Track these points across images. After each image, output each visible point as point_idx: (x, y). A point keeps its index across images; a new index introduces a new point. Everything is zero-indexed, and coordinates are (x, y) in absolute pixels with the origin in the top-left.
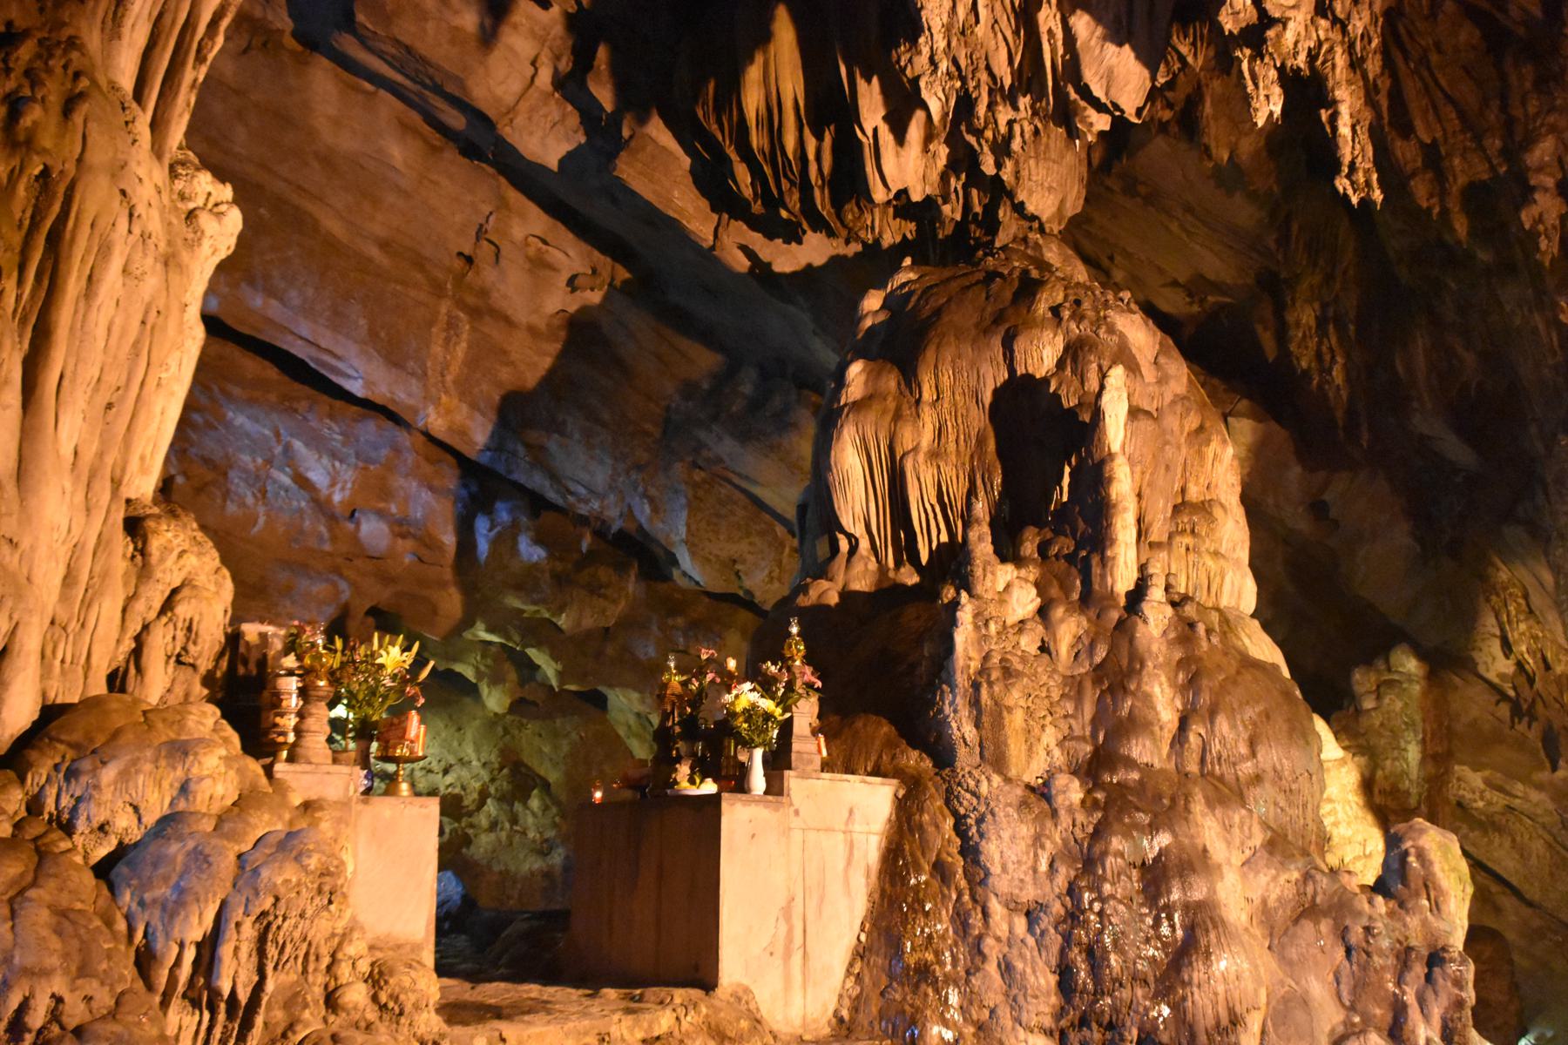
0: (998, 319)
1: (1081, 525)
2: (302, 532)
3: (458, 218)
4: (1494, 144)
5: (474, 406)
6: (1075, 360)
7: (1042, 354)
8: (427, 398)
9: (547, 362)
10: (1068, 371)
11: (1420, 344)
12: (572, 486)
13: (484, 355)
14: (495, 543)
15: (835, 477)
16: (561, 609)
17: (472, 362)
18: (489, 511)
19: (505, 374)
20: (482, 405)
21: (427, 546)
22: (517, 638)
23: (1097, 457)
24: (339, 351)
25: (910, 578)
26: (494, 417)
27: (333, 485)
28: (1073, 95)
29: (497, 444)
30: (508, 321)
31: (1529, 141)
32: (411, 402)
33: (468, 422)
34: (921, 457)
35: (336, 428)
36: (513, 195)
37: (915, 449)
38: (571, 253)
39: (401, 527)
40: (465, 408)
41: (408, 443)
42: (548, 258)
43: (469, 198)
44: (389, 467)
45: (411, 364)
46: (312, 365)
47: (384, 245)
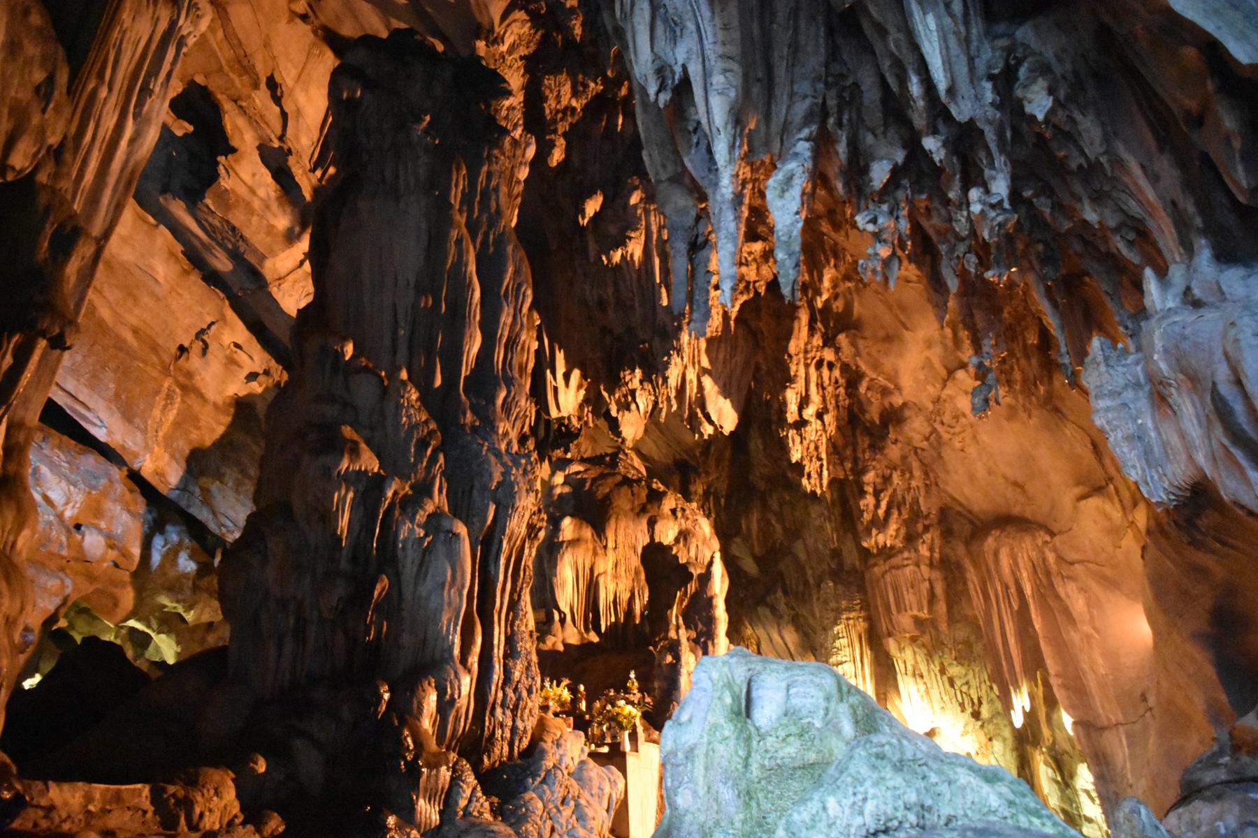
0: (643, 510)
1: (700, 626)
2: (49, 540)
3: (187, 321)
4: (848, 465)
5: (172, 456)
6: (685, 539)
7: (667, 533)
8: (147, 448)
9: (221, 430)
10: (681, 545)
11: (755, 516)
12: (224, 520)
13: (187, 420)
14: (165, 557)
15: (557, 581)
16: (189, 608)
17: (177, 425)
18: (162, 532)
19: (194, 436)
20: (177, 455)
21: (124, 556)
22: (155, 626)
23: (709, 594)
24: (91, 405)
25: (594, 638)
26: (184, 465)
27: (67, 503)
28: (700, 415)
29: (183, 487)
30: (201, 395)
31: (864, 471)
32: (135, 449)
33: (167, 468)
34: (609, 578)
35: (62, 457)
36: (230, 314)
37: (605, 573)
38: (255, 358)
39: (112, 542)
40: (167, 457)
41: (117, 477)
42: (235, 356)
43: (199, 309)
44: (104, 494)
45: (137, 420)
46: (68, 411)
47: (135, 332)
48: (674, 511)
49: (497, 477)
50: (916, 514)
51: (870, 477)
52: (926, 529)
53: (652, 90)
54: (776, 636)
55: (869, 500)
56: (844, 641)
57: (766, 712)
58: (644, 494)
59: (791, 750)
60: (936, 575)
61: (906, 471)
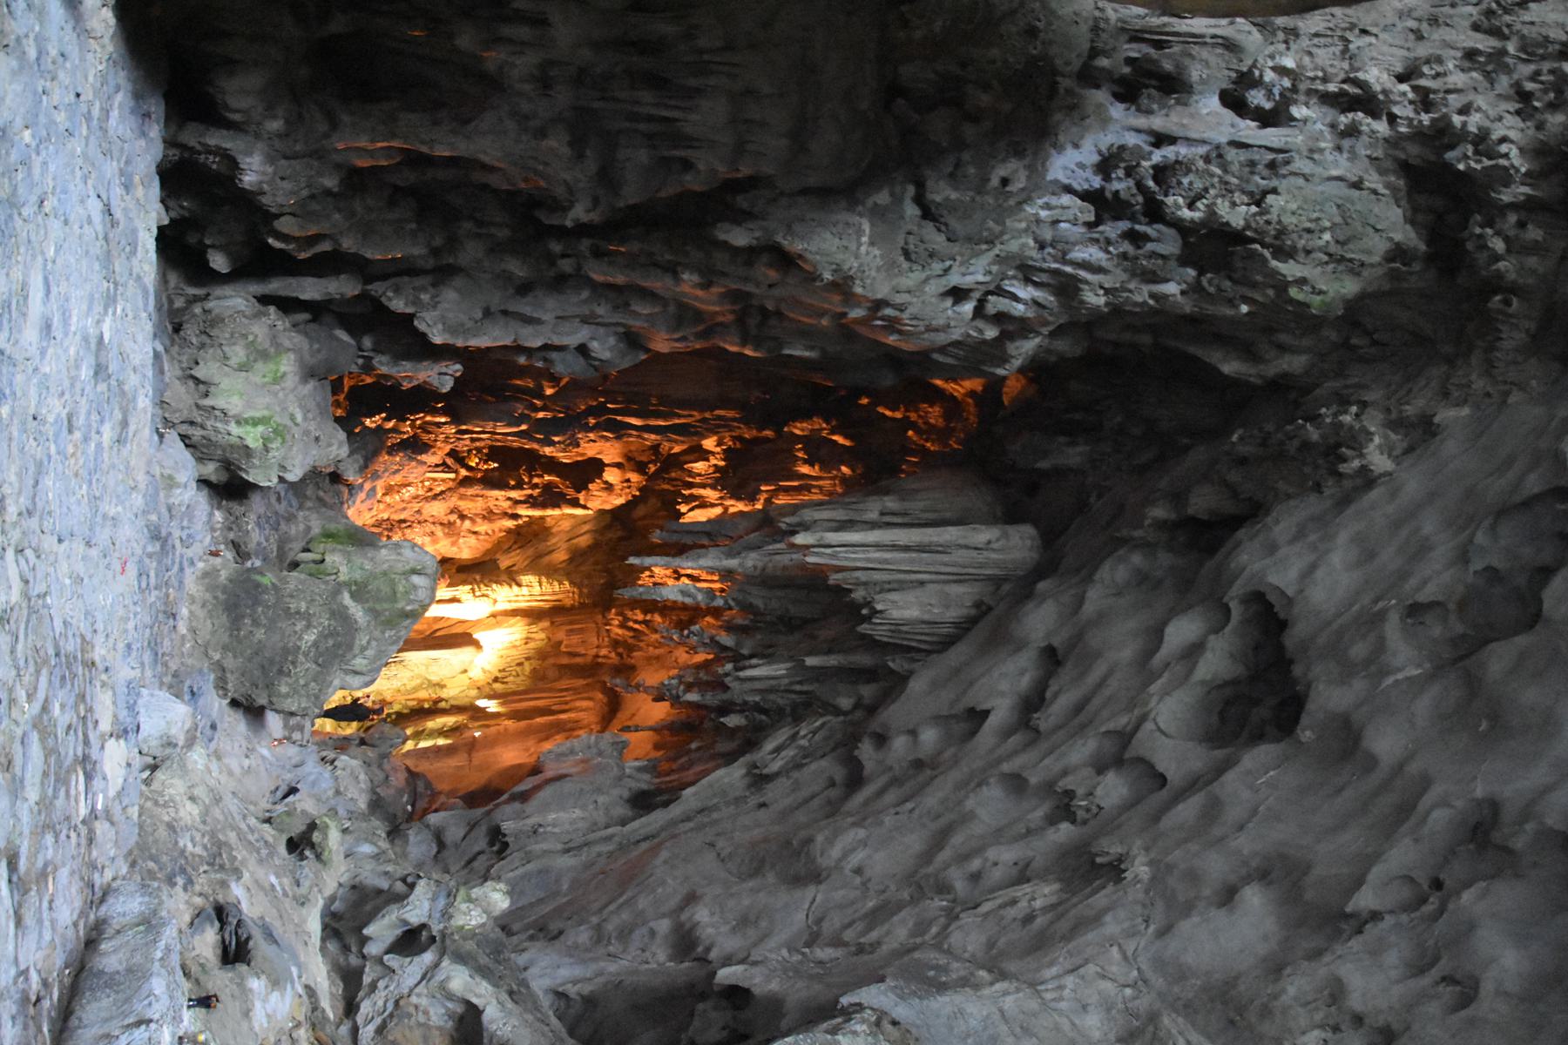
7: (611, 476)
31: (663, 615)
48: (628, 481)
49: (556, 439)
50: (631, 649)
51: (658, 618)
52: (620, 655)
53: (787, 520)
54: (586, 527)
55: (640, 617)
56: (557, 588)
57: (416, 579)
58: (644, 458)
59: (401, 589)
60: (589, 659)
61: (658, 645)
